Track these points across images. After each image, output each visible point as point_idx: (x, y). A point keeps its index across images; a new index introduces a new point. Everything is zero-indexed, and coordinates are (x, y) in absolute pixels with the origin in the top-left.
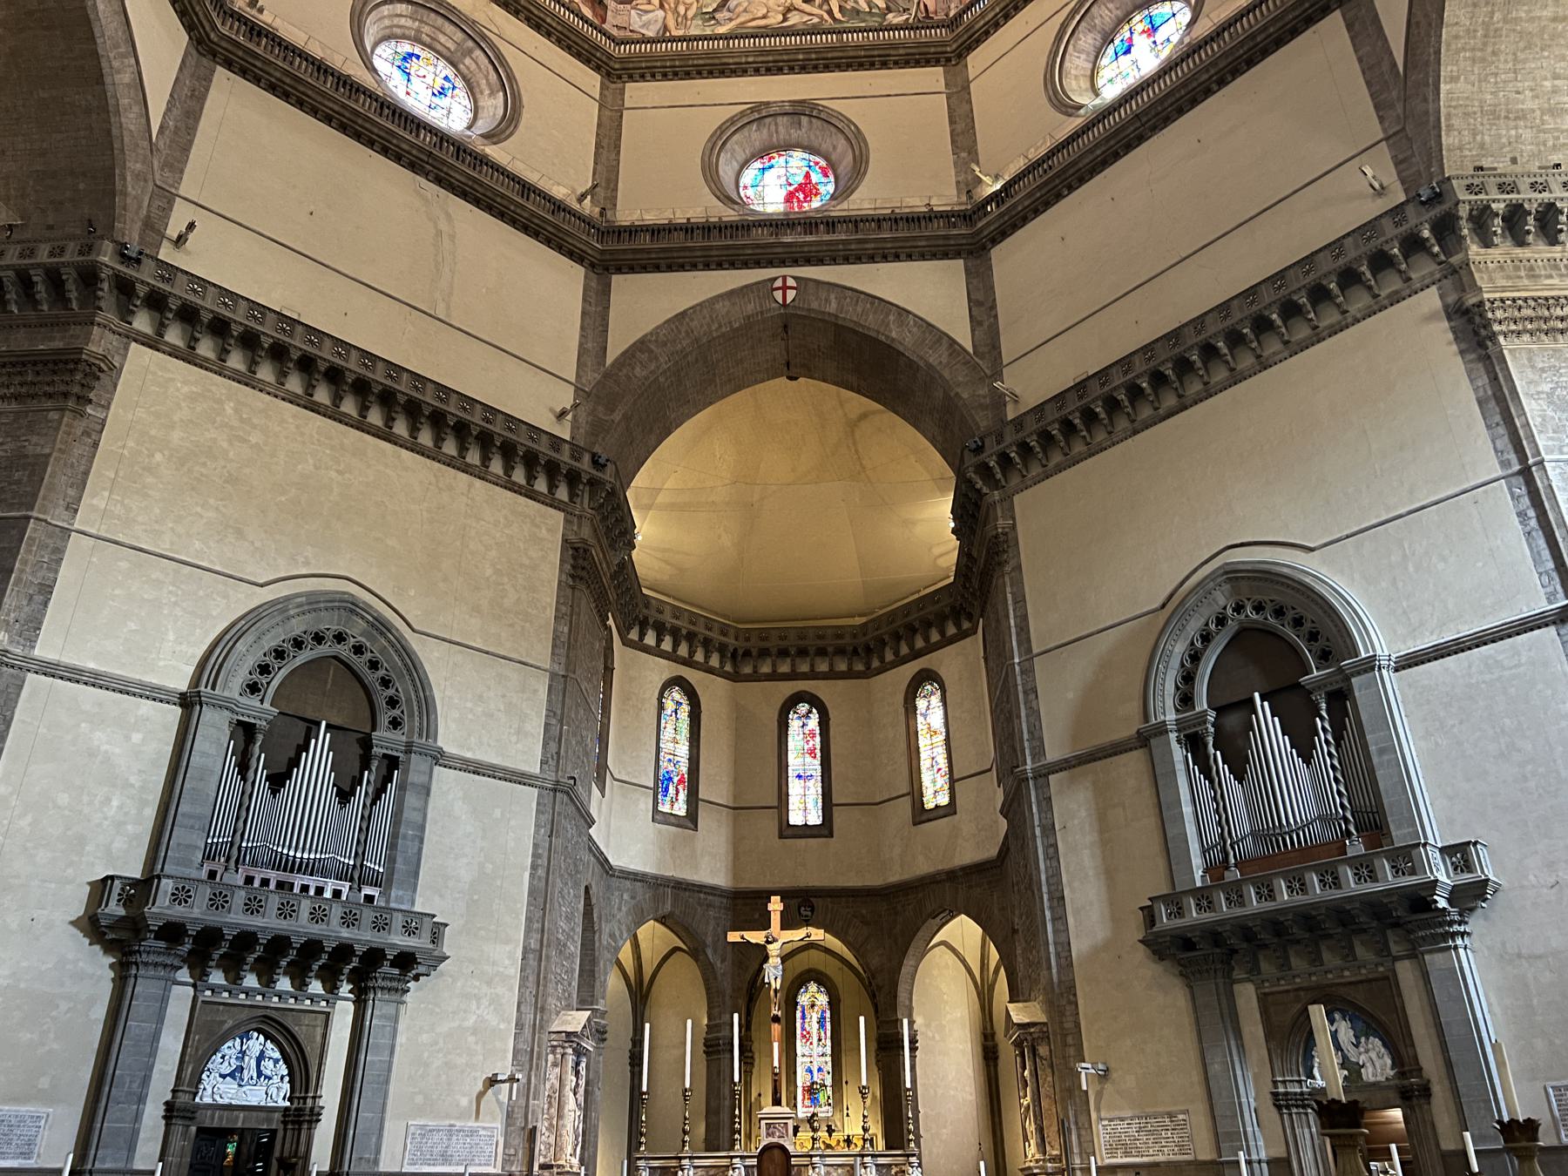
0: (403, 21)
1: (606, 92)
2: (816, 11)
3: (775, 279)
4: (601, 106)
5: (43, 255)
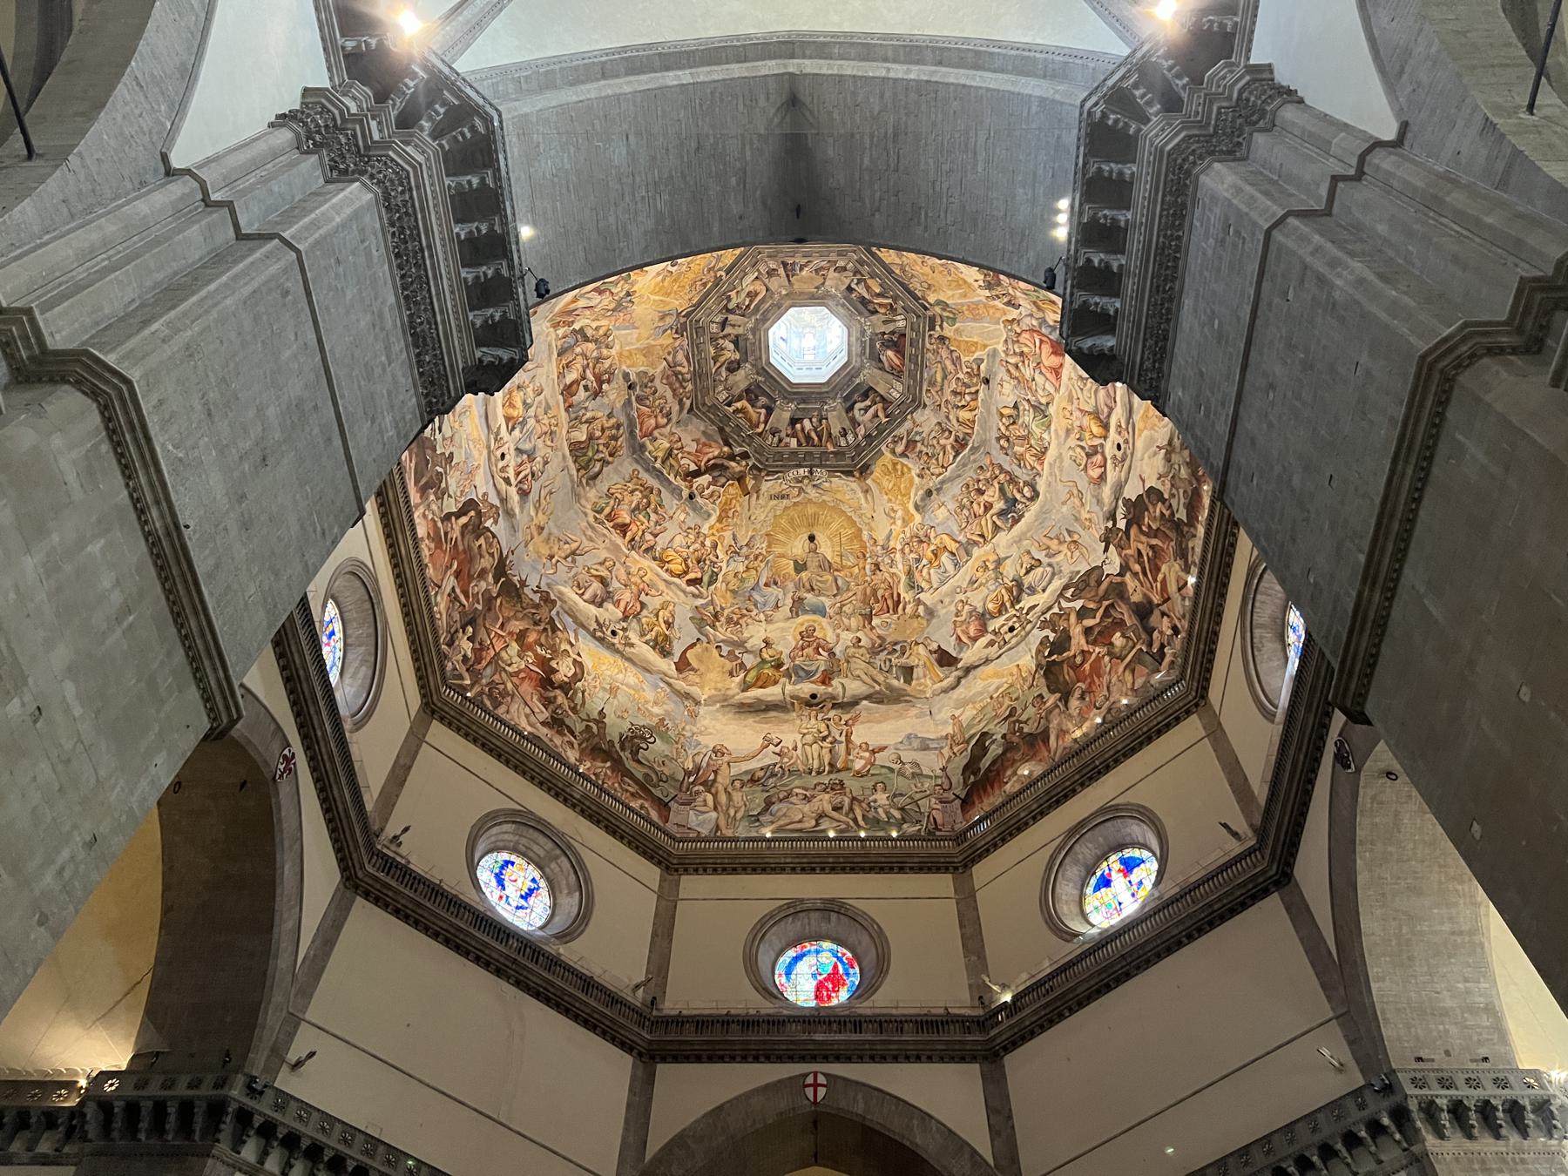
0: (506, 837)
1: (666, 884)
2: (843, 818)
3: (806, 1075)
4: (659, 896)
5: (181, 1090)
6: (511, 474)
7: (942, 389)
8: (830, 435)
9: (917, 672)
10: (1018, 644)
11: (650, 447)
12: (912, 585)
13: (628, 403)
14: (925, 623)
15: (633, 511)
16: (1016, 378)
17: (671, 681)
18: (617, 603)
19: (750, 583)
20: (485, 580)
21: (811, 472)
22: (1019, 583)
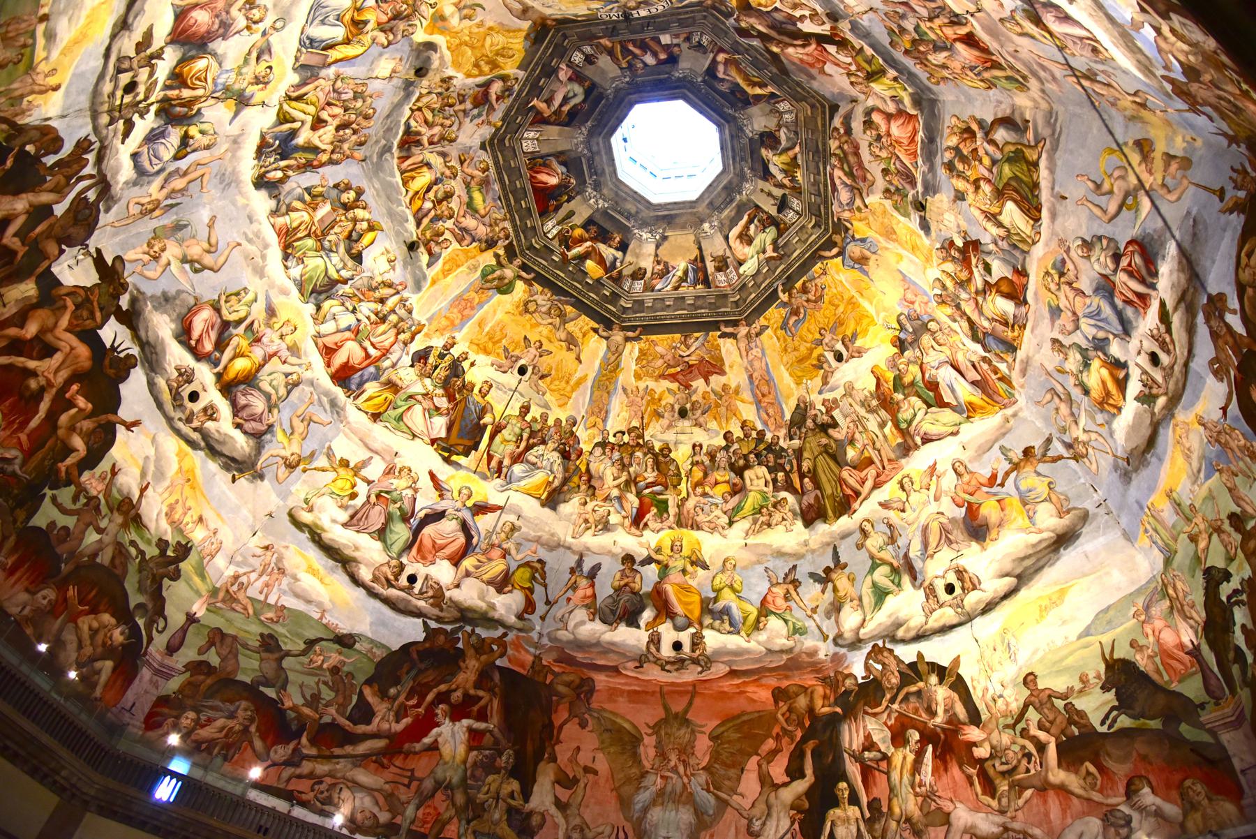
7: (468, 186)
8: (611, 52)
10: (96, 92)
13: (931, 188)
15: (945, 48)
16: (377, 288)
21: (627, 17)
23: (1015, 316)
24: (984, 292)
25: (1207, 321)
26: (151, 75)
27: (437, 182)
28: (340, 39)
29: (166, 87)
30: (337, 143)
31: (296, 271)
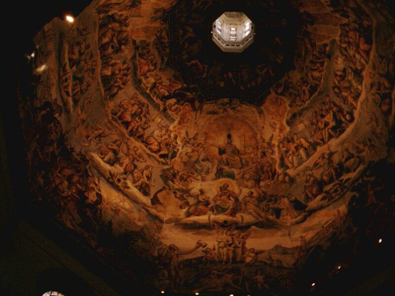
6: (70, 90)
9: (284, 212)
10: (339, 199)
11: (144, 81)
12: (283, 165)
13: (134, 57)
14: (288, 185)
16: (345, 55)
17: (149, 209)
18: (121, 165)
19: (194, 159)
20: (53, 146)
22: (341, 165)
23: (102, 40)
24: (112, 38)
25: (61, 107)
26: (331, 189)
27: (312, 70)
28: (303, 149)
29: (334, 182)
30: (328, 111)
31: (359, 87)
